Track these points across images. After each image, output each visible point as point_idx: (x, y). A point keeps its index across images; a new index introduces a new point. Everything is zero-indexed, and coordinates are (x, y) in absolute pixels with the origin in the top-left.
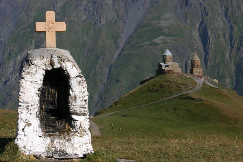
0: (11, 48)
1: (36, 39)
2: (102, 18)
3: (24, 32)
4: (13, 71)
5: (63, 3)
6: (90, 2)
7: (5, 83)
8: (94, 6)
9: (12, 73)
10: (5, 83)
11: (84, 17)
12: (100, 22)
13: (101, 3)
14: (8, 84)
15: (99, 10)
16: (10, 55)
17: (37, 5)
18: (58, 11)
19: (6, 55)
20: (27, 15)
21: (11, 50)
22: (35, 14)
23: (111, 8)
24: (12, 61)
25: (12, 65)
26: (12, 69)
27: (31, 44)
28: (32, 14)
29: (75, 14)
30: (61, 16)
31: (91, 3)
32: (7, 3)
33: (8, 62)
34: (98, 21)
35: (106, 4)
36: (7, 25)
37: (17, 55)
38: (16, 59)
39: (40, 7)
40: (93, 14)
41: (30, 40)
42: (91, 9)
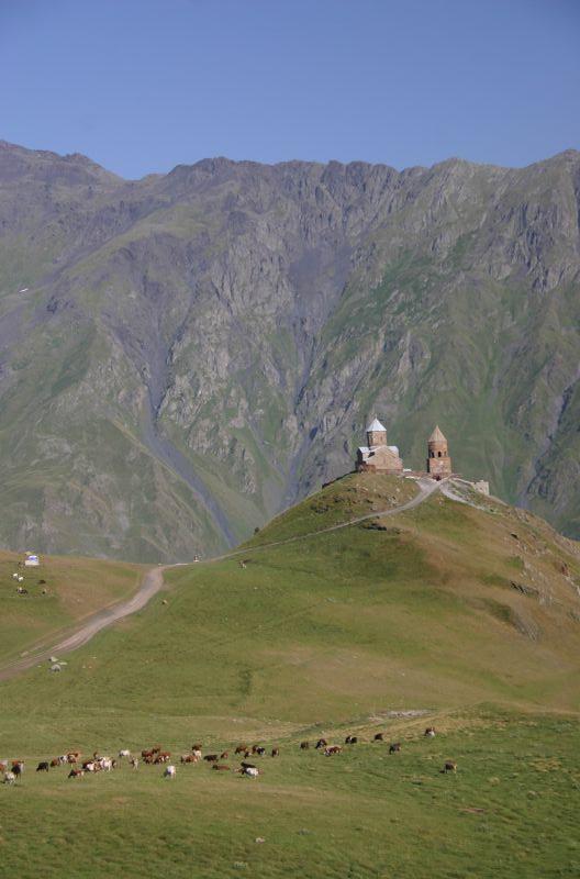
0: (329, 348)
1: (389, 326)
2: (550, 273)
3: (361, 310)
4: (332, 404)
5: (457, 237)
6: (521, 234)
7: (313, 433)
8: (532, 243)
9: (329, 410)
10: (313, 433)
11: (507, 271)
12: (545, 283)
13: (549, 234)
14: (319, 435)
15: (544, 252)
16: (325, 365)
17: (393, 242)
18: (444, 257)
19: (317, 365)
20: (369, 268)
21: (328, 354)
22: (388, 266)
23: (574, 246)
24: (329, 380)
25: (329, 390)
26: (330, 400)
27: (377, 338)
28: (382, 265)
29: (485, 265)
30: (450, 270)
31: (525, 235)
32: (322, 238)
33: (321, 383)
34: (541, 282)
35: (563, 238)
36: (321, 293)
37: (341, 367)
38: (339, 375)
39: (401, 248)
40: (529, 264)
41: (375, 328)
42: (525, 252)
